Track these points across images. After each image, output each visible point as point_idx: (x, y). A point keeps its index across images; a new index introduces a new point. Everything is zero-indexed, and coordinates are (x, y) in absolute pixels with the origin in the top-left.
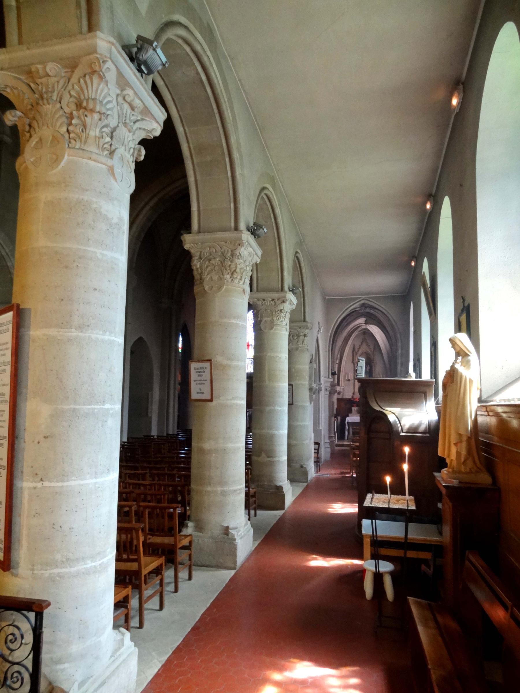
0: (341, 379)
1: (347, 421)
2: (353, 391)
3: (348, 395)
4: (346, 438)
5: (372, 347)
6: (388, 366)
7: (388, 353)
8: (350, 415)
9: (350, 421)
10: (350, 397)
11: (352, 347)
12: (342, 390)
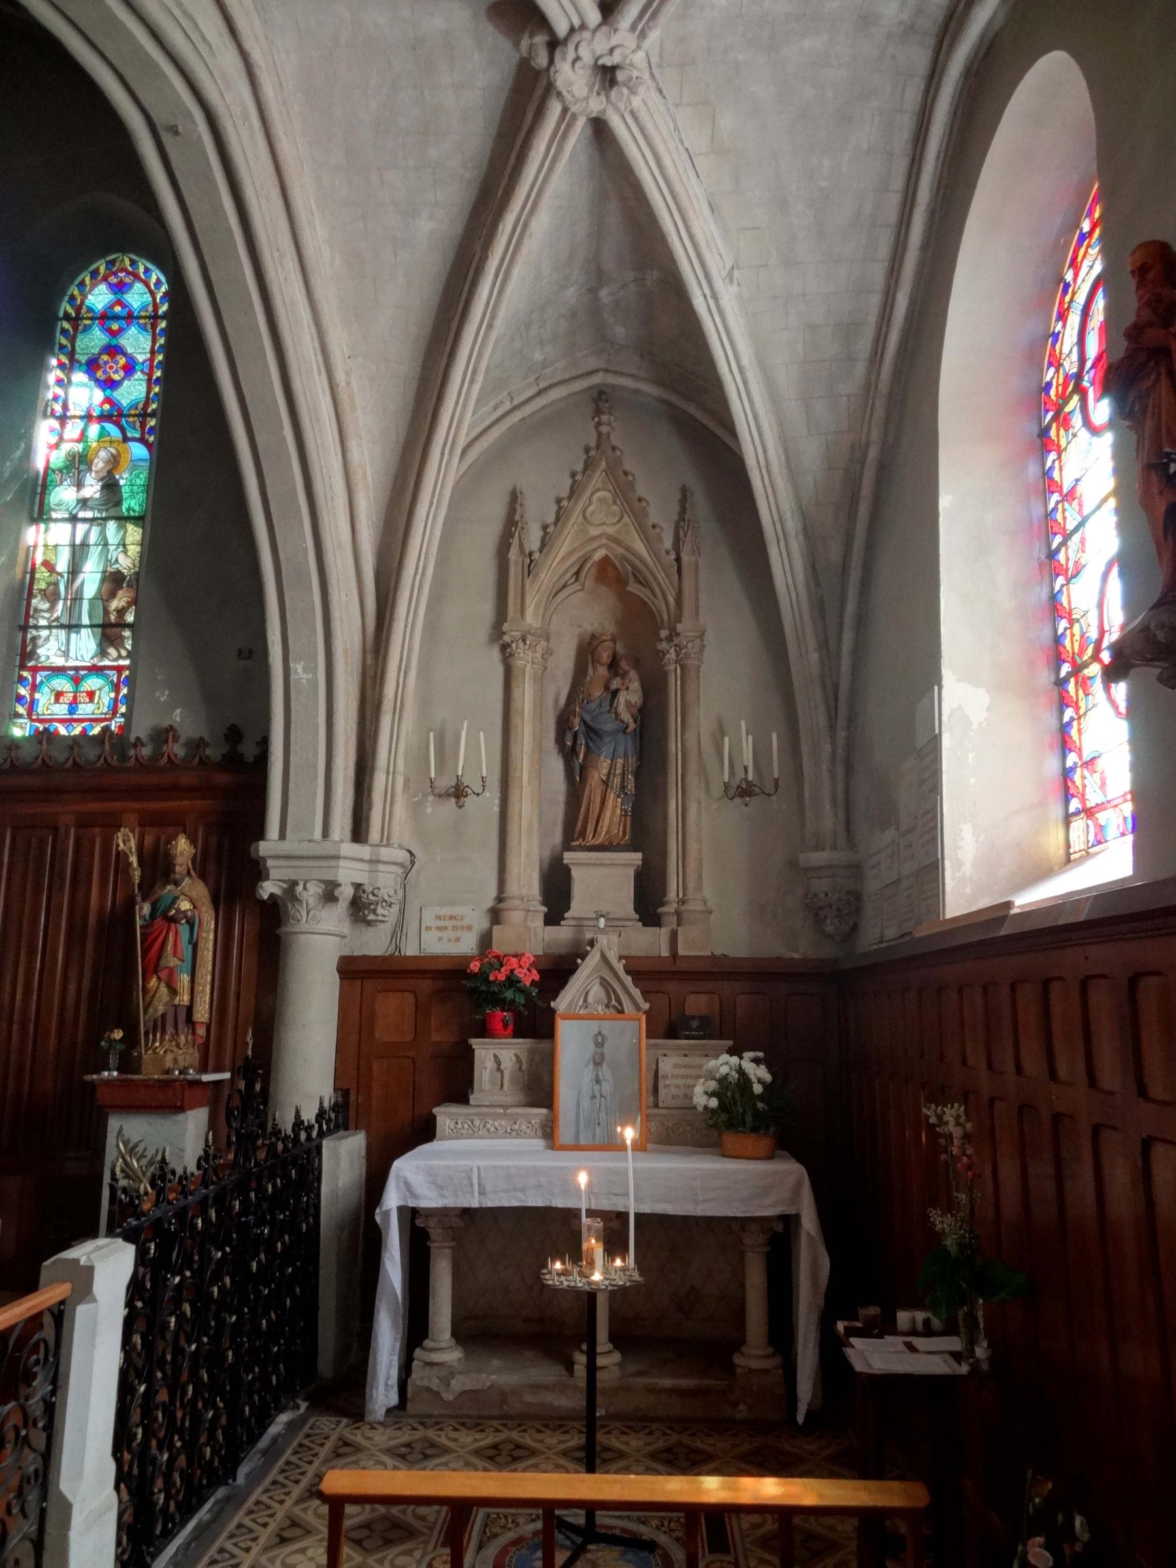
0: (379, 781)
1: (392, 1199)
2: (493, 892)
3: (444, 930)
4: (383, 1393)
5: (661, 514)
6: (805, 659)
7: (808, 532)
8: (446, 1116)
9: (429, 1199)
10: (467, 945)
11: (496, 510)
12: (386, 882)
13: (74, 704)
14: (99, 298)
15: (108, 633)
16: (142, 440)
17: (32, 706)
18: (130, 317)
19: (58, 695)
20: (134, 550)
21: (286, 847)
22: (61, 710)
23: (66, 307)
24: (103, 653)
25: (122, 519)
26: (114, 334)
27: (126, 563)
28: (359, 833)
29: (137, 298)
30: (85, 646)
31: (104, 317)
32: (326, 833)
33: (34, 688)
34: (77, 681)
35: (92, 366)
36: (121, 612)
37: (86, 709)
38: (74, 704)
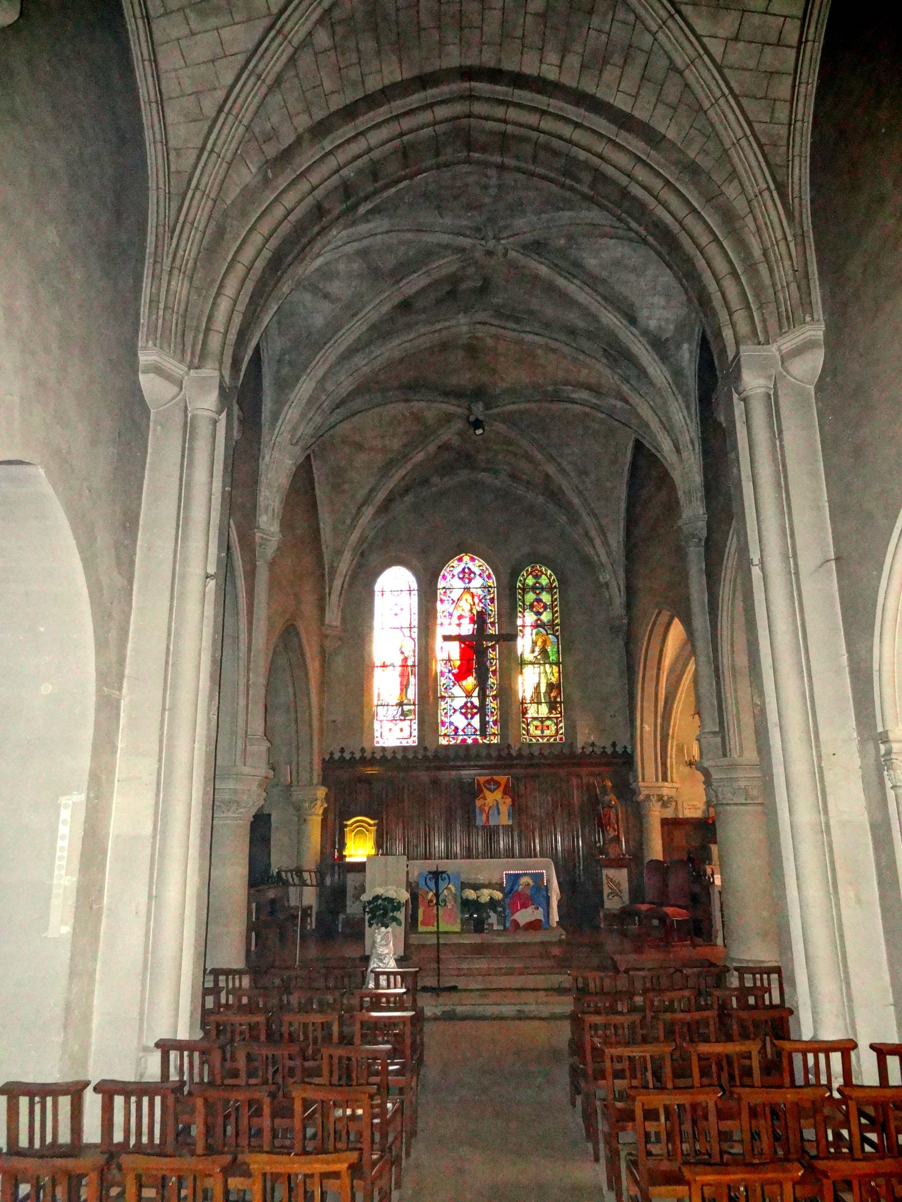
13: (542, 731)
14: (530, 581)
15: (552, 706)
16: (553, 635)
17: (528, 731)
18: (542, 589)
19: (536, 727)
20: (556, 675)
21: (645, 784)
22: (538, 732)
23: (519, 584)
24: (550, 712)
25: (551, 664)
26: (538, 594)
27: (554, 680)
28: (665, 779)
29: (544, 581)
30: (544, 710)
31: (533, 588)
32: (657, 780)
33: (528, 725)
34: (542, 722)
35: (532, 606)
36: (555, 697)
37: (547, 732)
38: (542, 731)
